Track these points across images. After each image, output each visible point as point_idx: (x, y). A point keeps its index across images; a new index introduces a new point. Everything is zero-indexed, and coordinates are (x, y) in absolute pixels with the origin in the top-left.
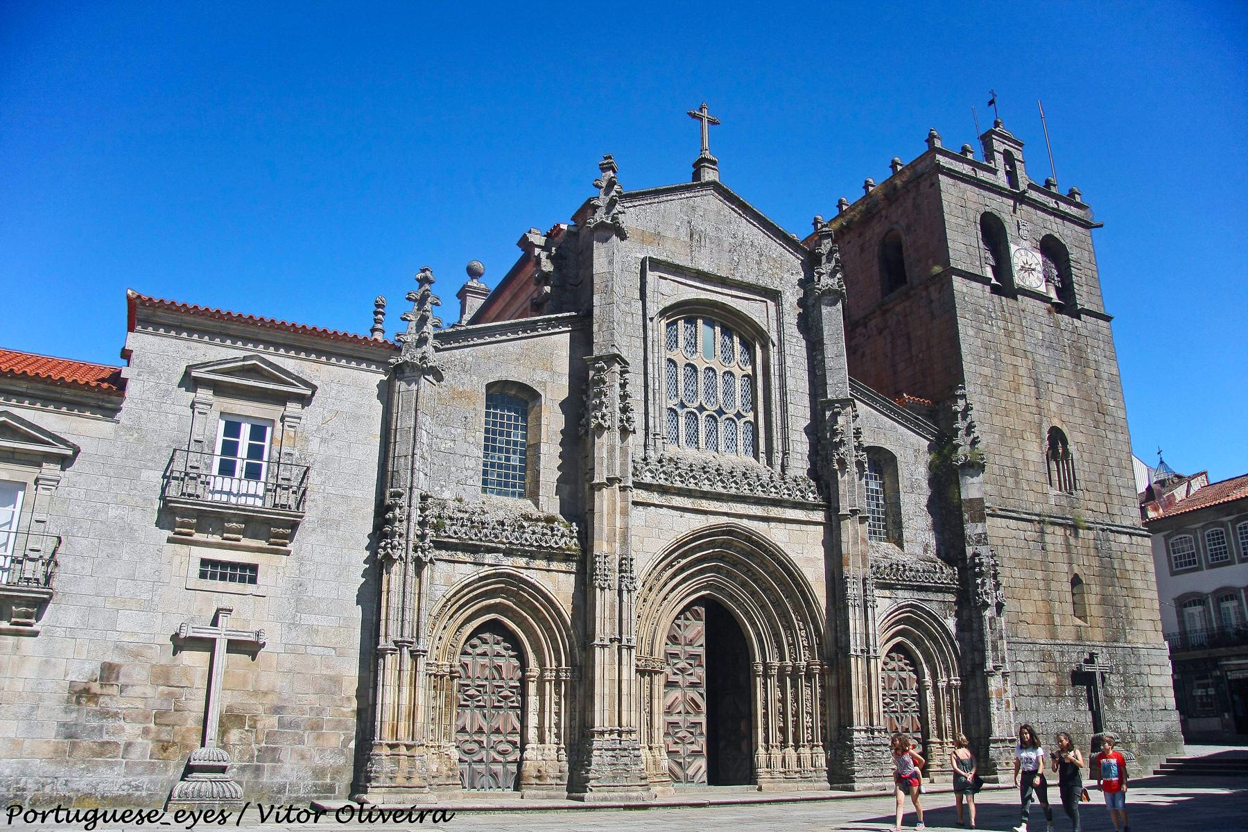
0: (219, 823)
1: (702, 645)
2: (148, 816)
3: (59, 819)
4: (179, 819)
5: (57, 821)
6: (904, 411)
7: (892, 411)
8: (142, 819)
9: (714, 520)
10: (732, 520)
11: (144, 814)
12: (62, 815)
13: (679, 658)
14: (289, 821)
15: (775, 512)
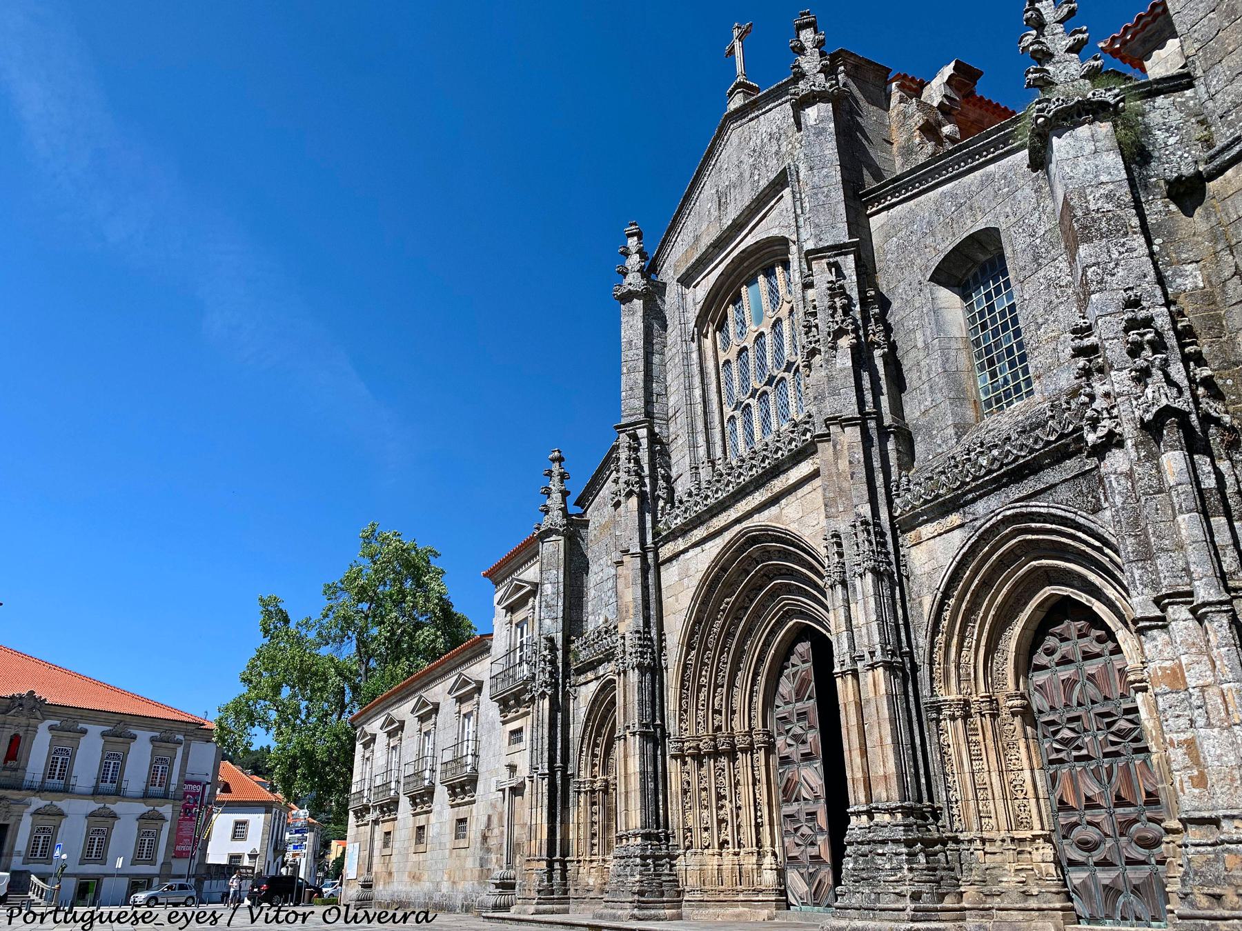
0: (132, 923)
1: (810, 698)
2: (143, 917)
3: (58, 920)
4: (173, 920)
5: (55, 922)
6: (990, 134)
7: (972, 155)
8: (137, 920)
9: (728, 536)
10: (737, 528)
11: (138, 915)
12: (60, 916)
13: (790, 722)
14: (278, 922)
15: (778, 484)
